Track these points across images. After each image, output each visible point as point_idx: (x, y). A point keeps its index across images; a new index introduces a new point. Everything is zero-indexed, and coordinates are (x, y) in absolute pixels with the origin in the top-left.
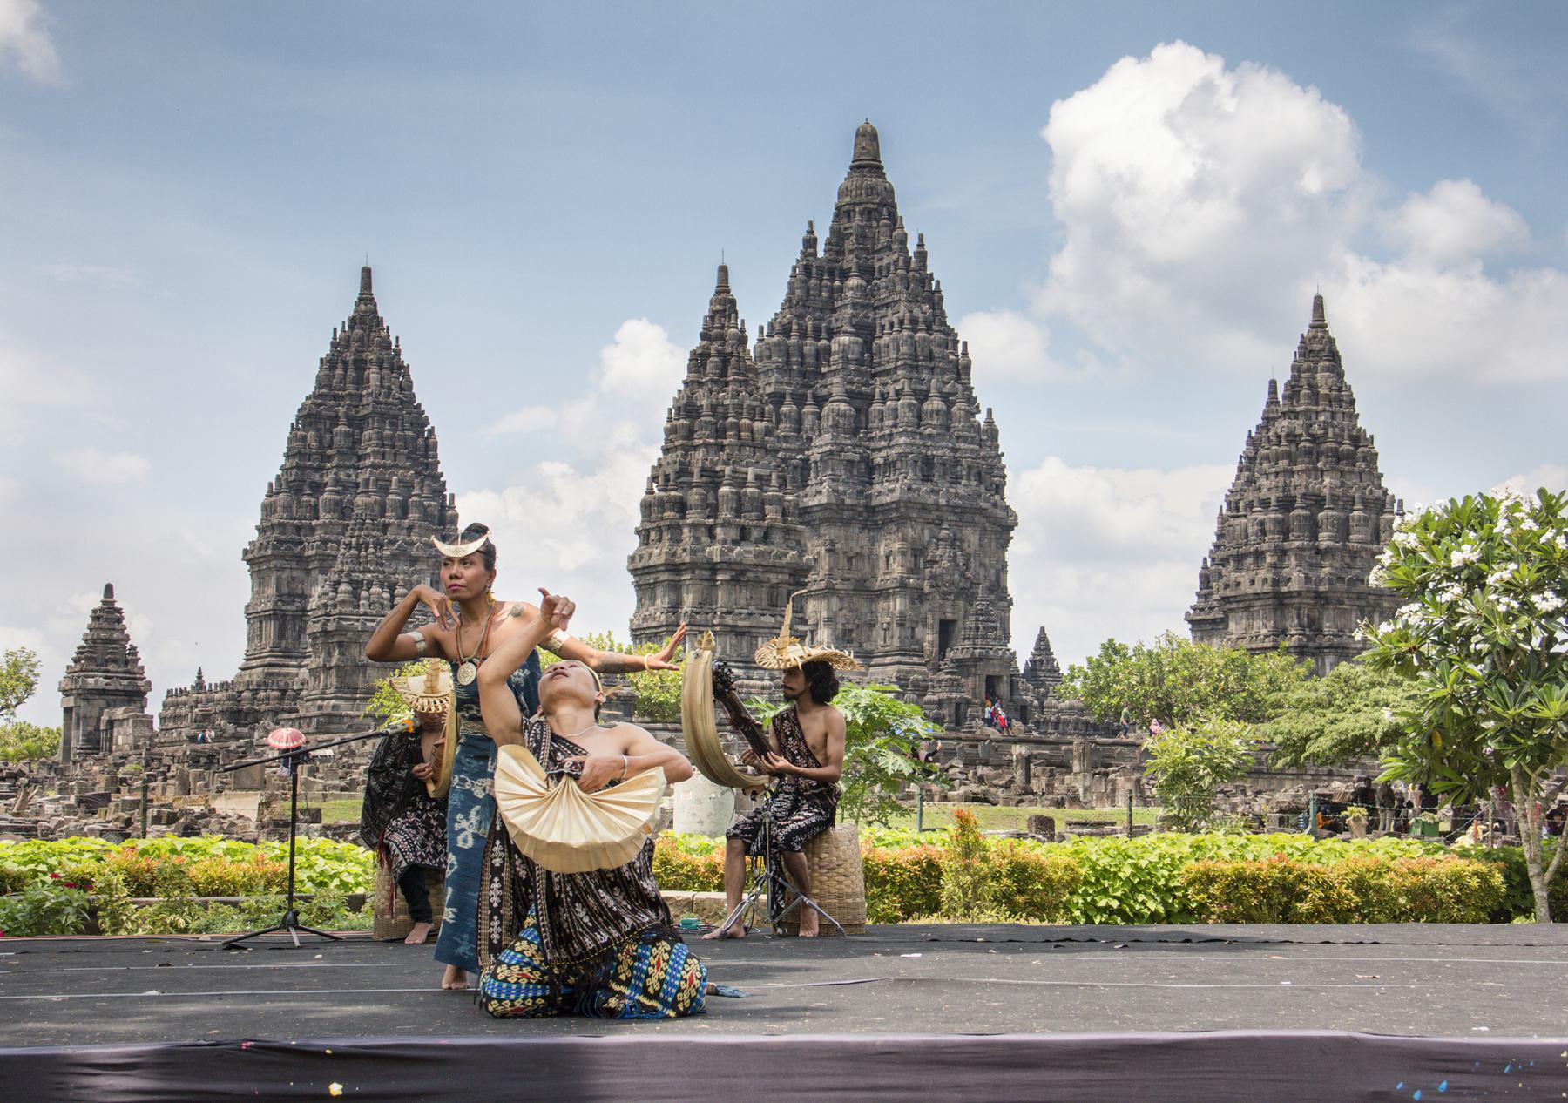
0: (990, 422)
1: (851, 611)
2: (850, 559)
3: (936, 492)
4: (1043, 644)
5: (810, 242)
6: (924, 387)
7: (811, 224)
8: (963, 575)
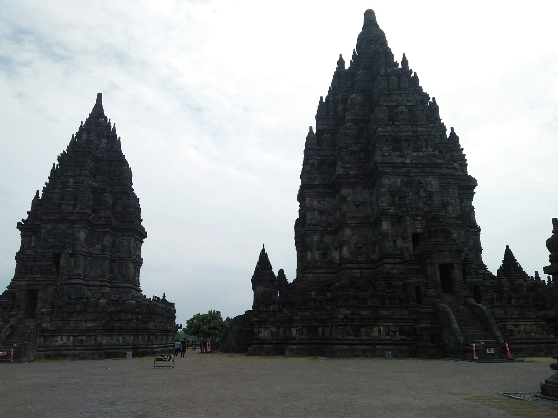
0: (453, 133)
1: (359, 236)
2: (357, 206)
3: (404, 156)
4: (508, 254)
5: (341, 62)
6: (394, 104)
7: (341, 55)
8: (426, 203)
